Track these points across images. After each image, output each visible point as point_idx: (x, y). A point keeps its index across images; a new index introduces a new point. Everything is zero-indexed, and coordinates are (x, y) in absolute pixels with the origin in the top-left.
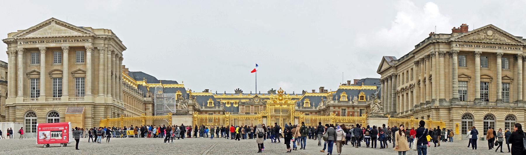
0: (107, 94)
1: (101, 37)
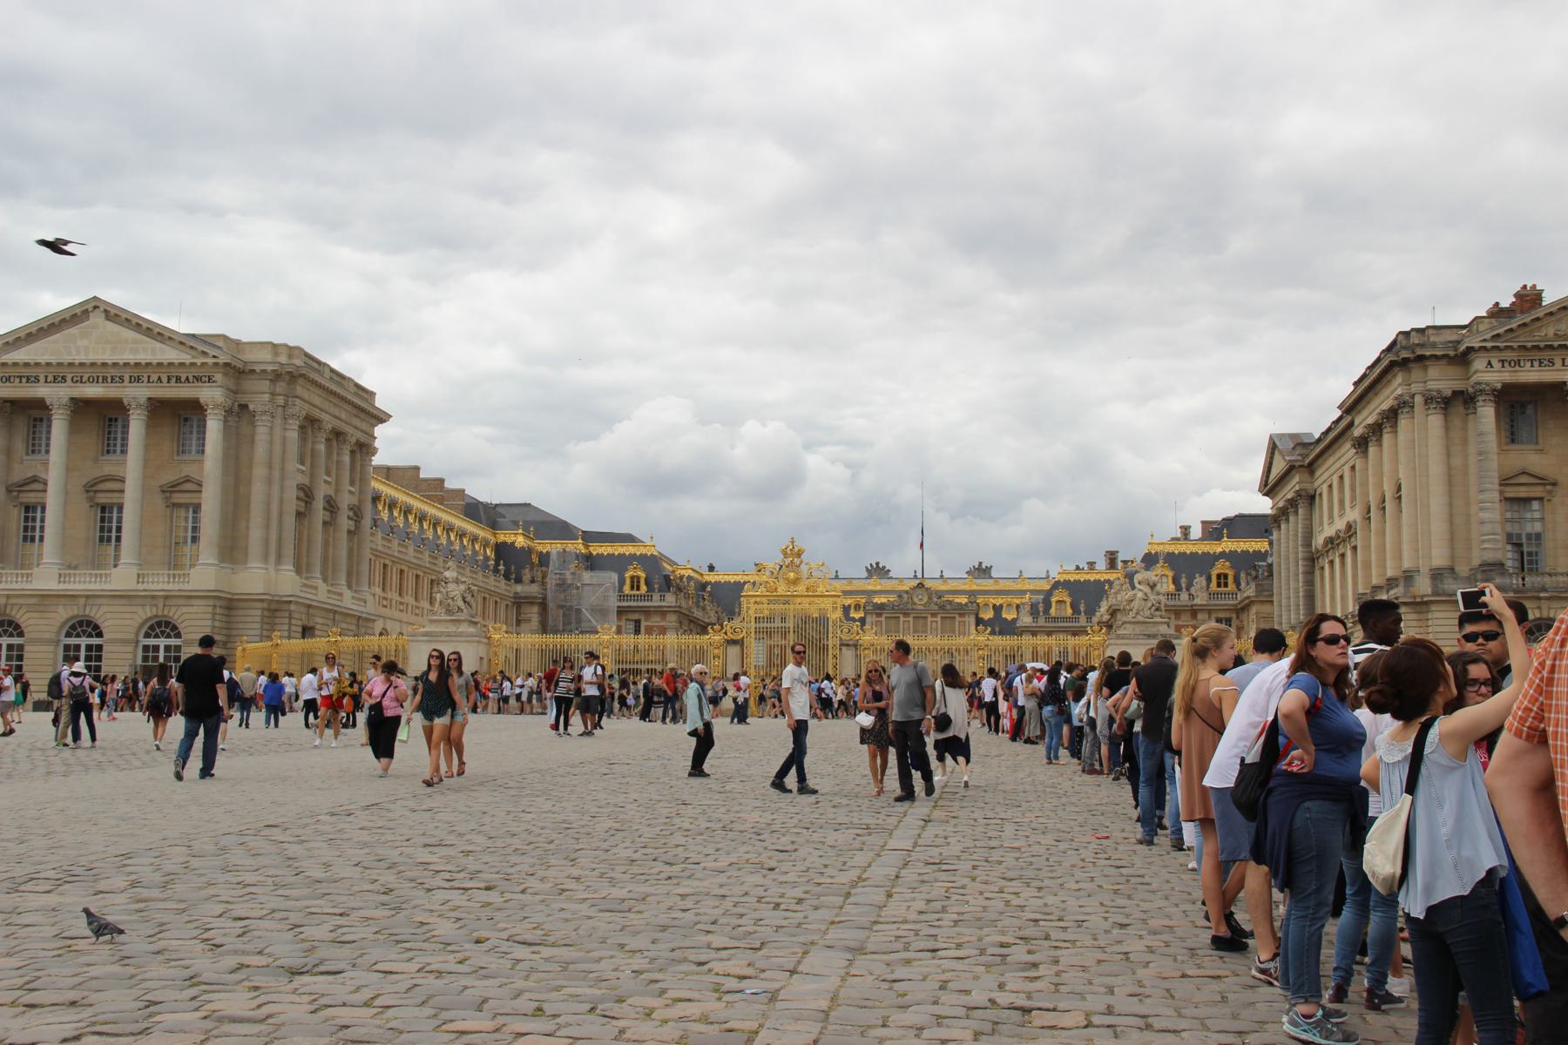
0: (279, 559)
1: (258, 368)
